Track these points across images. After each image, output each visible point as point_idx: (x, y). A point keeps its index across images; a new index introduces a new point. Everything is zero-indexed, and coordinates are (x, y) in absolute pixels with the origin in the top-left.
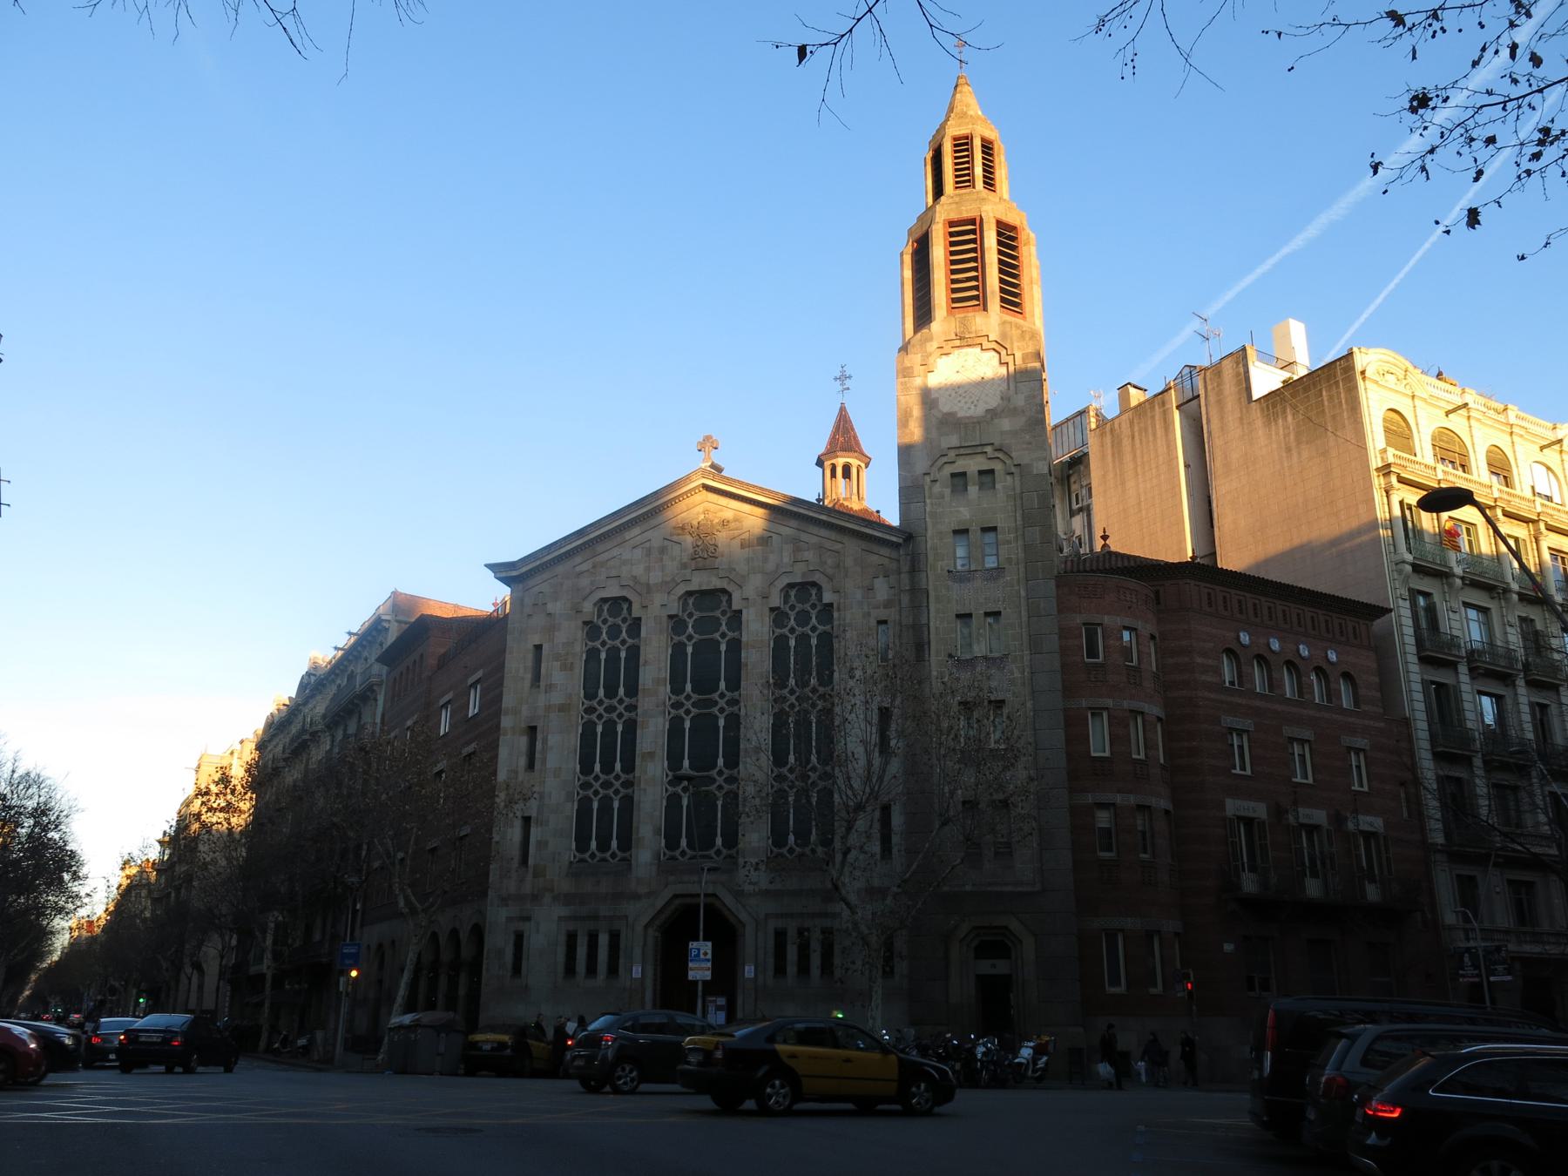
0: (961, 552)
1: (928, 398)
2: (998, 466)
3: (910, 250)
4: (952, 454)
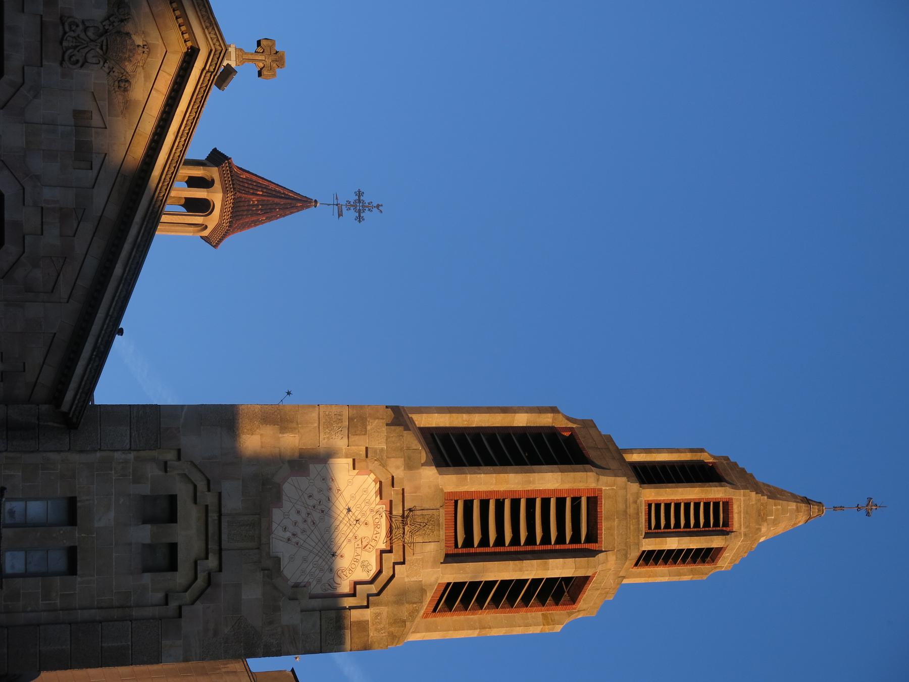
0: (36, 509)
1: (311, 464)
2: (181, 577)
3: (560, 422)
4: (210, 499)
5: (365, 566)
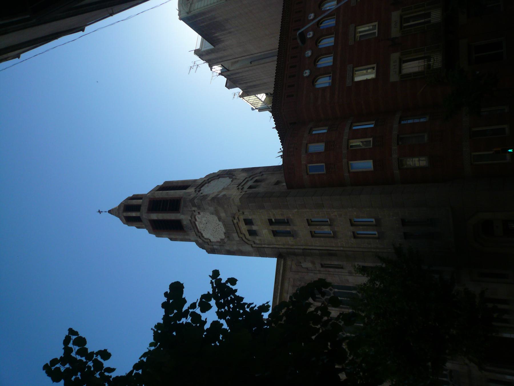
2: (242, 217)
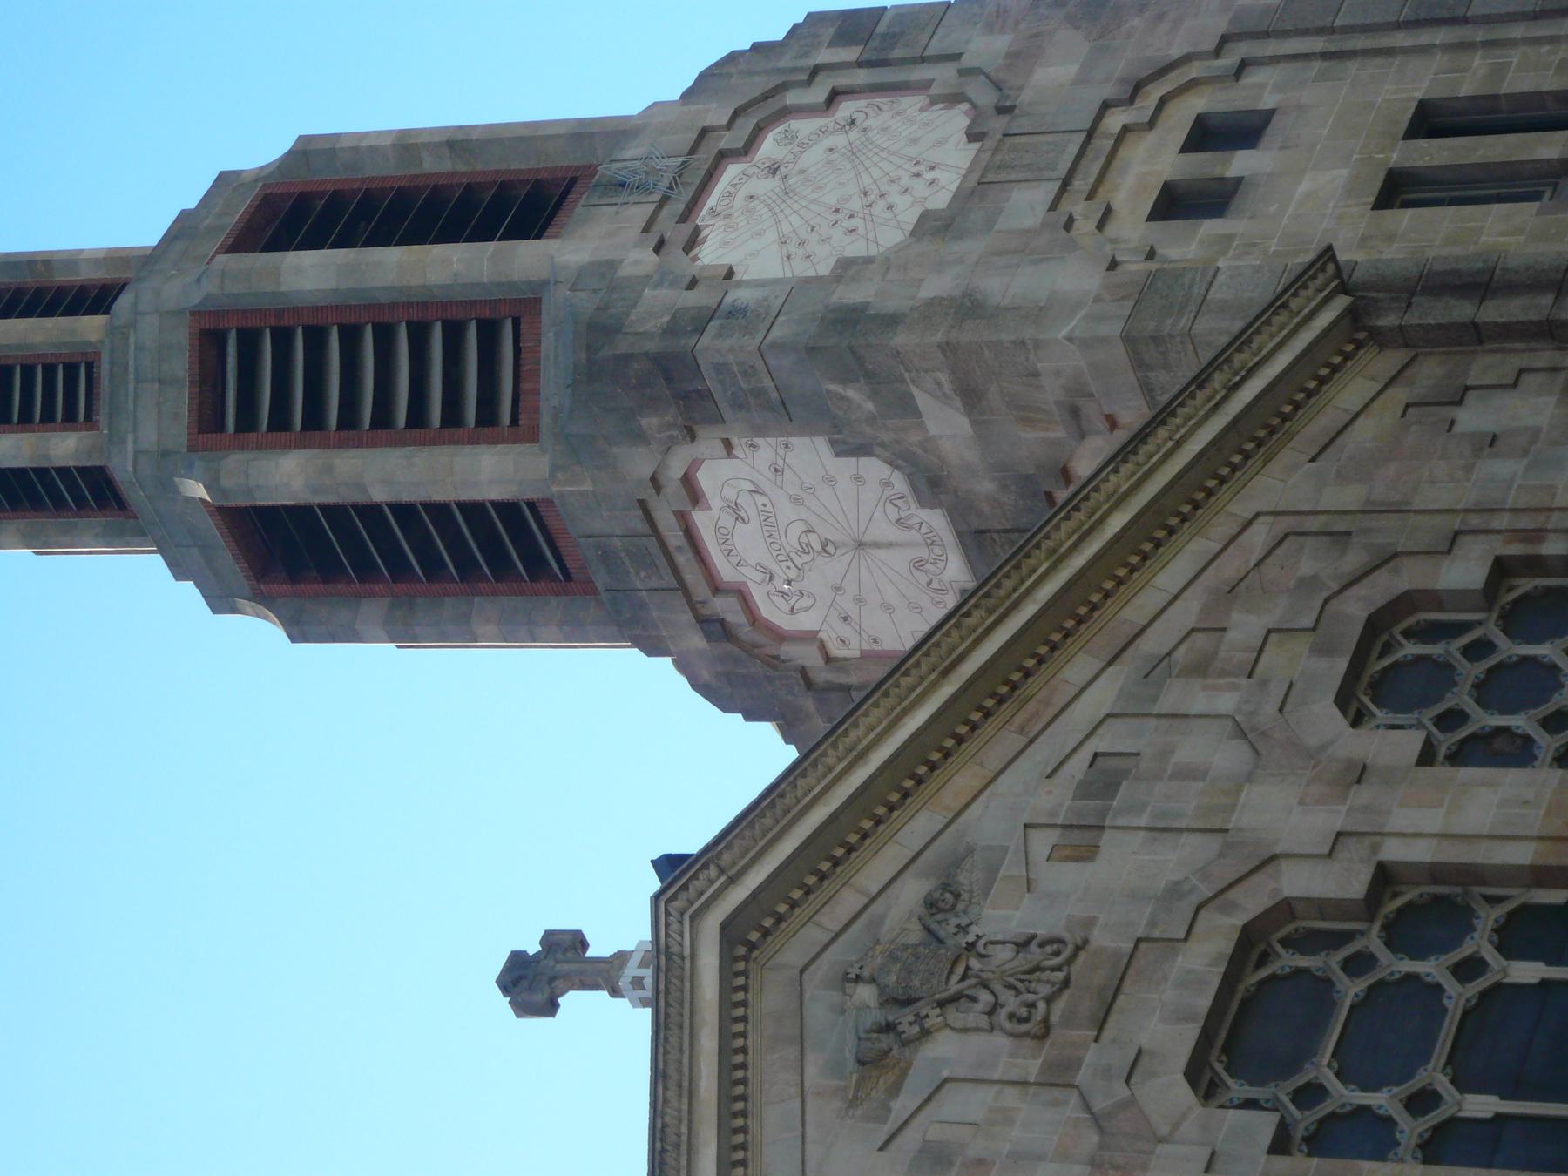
4: (1076, 205)
5: (790, 138)
